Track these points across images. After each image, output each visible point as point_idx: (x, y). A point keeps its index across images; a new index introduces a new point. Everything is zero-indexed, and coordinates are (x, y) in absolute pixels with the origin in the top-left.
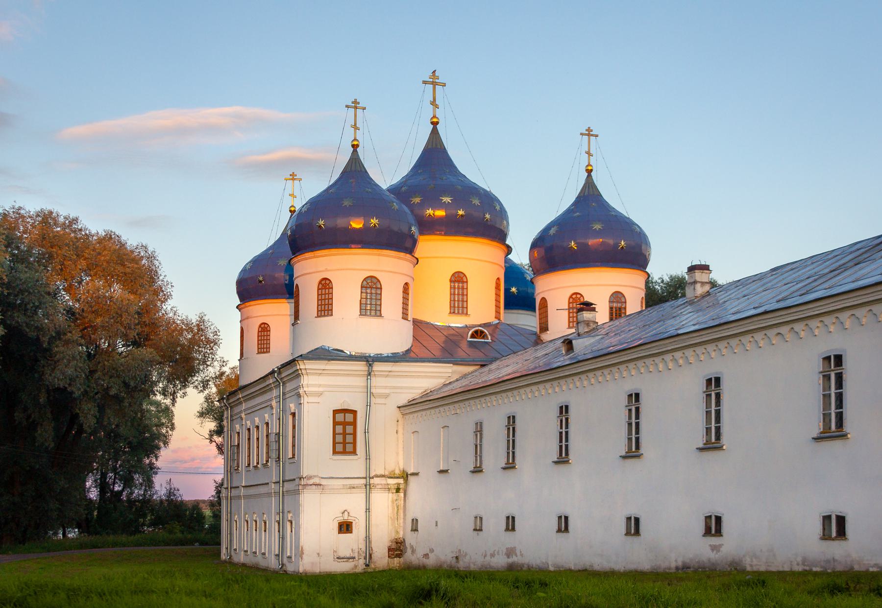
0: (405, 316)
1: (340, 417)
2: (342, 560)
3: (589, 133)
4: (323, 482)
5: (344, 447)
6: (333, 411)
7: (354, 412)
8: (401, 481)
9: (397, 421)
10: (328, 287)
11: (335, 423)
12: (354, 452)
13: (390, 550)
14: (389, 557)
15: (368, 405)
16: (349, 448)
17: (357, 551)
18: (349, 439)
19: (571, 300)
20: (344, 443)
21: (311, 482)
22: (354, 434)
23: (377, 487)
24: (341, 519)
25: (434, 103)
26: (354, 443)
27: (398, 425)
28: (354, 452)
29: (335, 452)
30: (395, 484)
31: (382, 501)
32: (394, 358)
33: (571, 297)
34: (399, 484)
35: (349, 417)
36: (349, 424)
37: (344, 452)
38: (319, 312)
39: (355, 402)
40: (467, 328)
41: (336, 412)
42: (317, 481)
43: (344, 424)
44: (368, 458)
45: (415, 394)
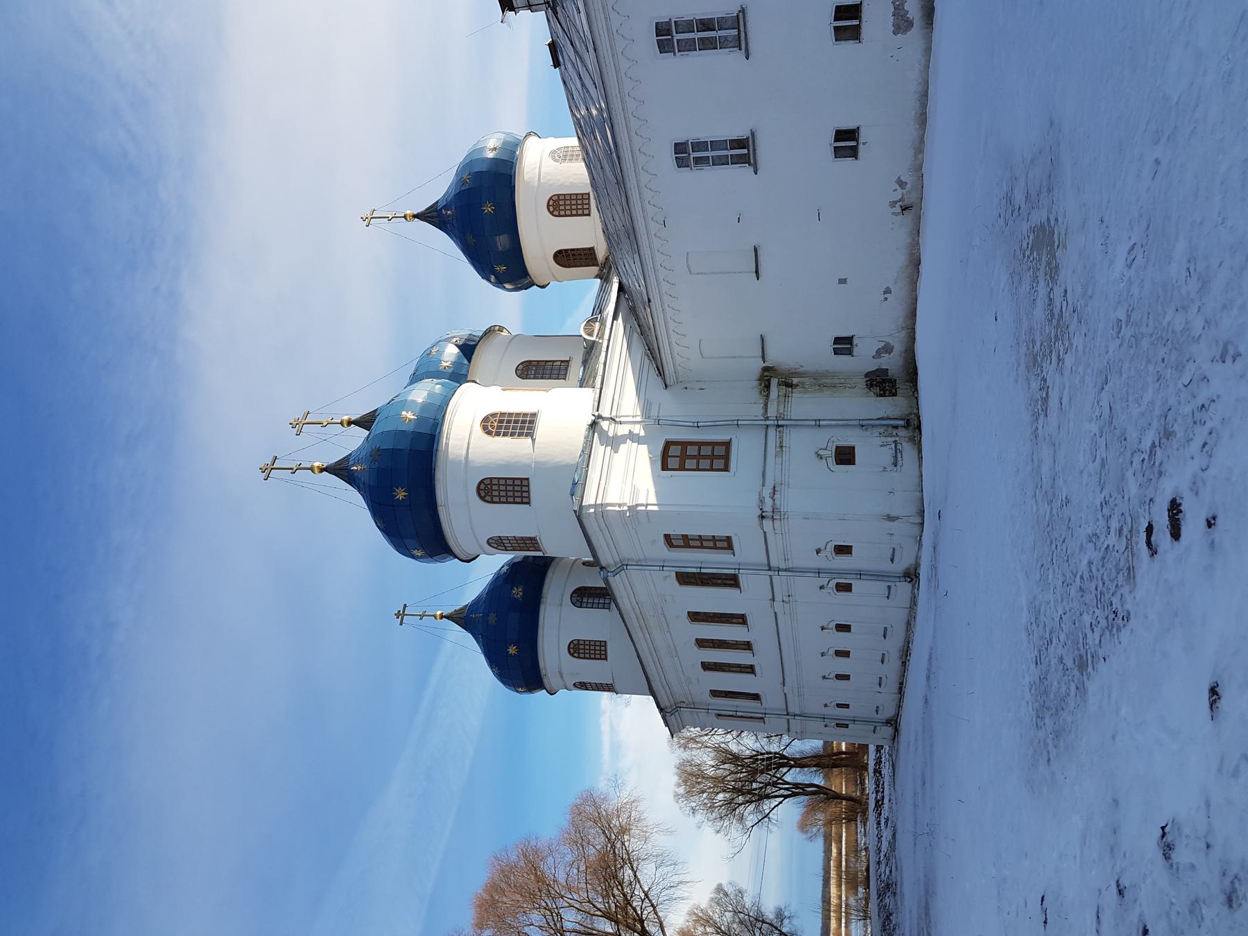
2: (899, 459)
4: (770, 483)
5: (719, 457)
6: (663, 470)
7: (668, 444)
8: (774, 382)
9: (686, 388)
10: (489, 486)
11: (682, 468)
13: (882, 395)
14: (894, 395)
16: (720, 451)
17: (883, 439)
18: (706, 451)
20: (712, 457)
21: (769, 502)
22: (700, 444)
23: (782, 411)
24: (831, 461)
26: (713, 444)
27: (692, 389)
28: (727, 445)
29: (726, 469)
30: (778, 388)
31: (802, 405)
34: (779, 384)
35: (676, 450)
36: (684, 451)
37: (727, 457)
38: (525, 500)
42: (767, 492)
43: (684, 457)
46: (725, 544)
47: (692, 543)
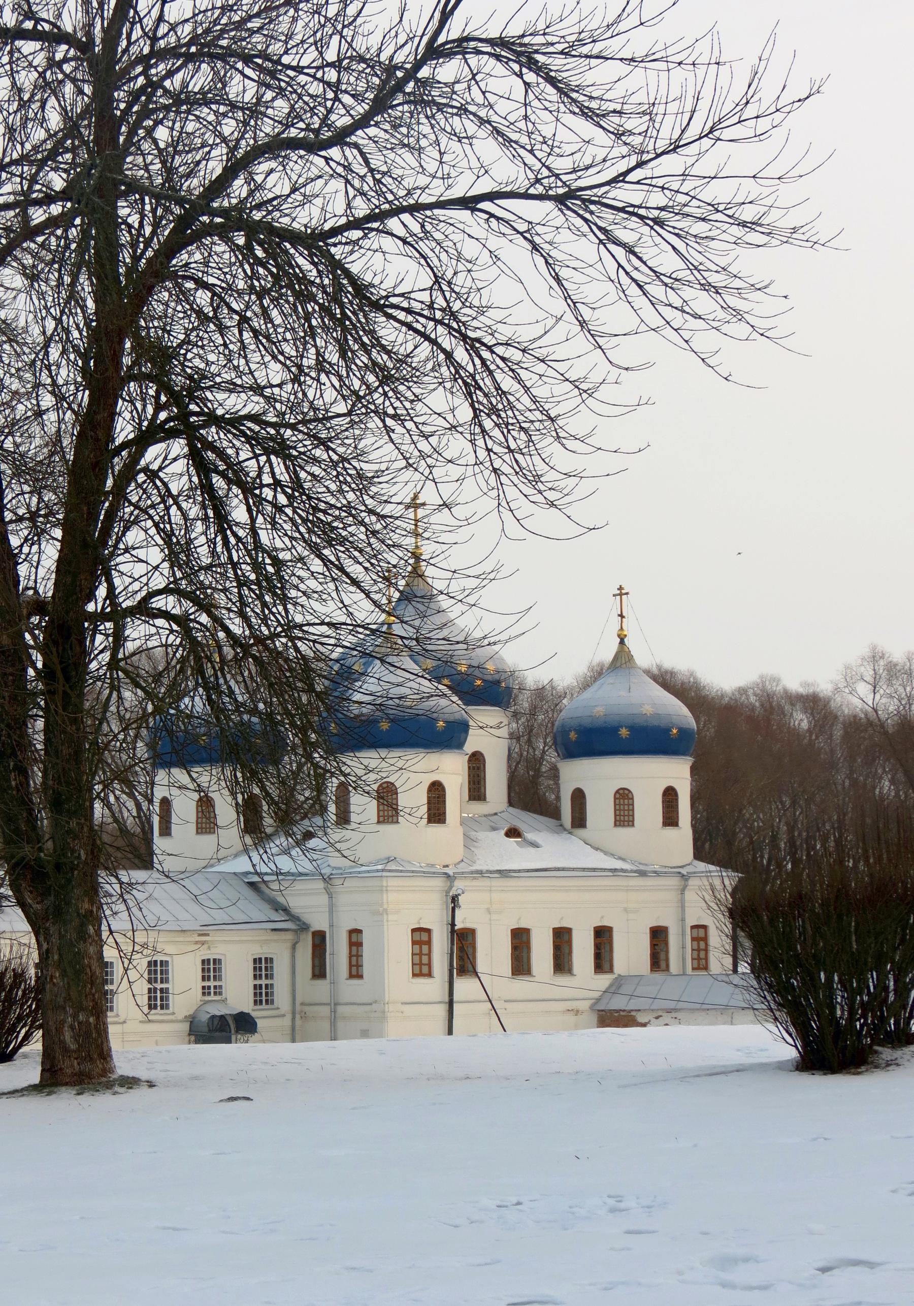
3: (621, 593)
7: (428, 931)
11: (414, 943)
12: (429, 975)
16: (425, 970)
18: (425, 959)
19: (618, 796)
20: (421, 964)
22: (429, 954)
26: (429, 965)
28: (429, 975)
29: (414, 975)
33: (617, 792)
35: (425, 937)
41: (413, 930)
46: (354, 972)
47: (354, 948)
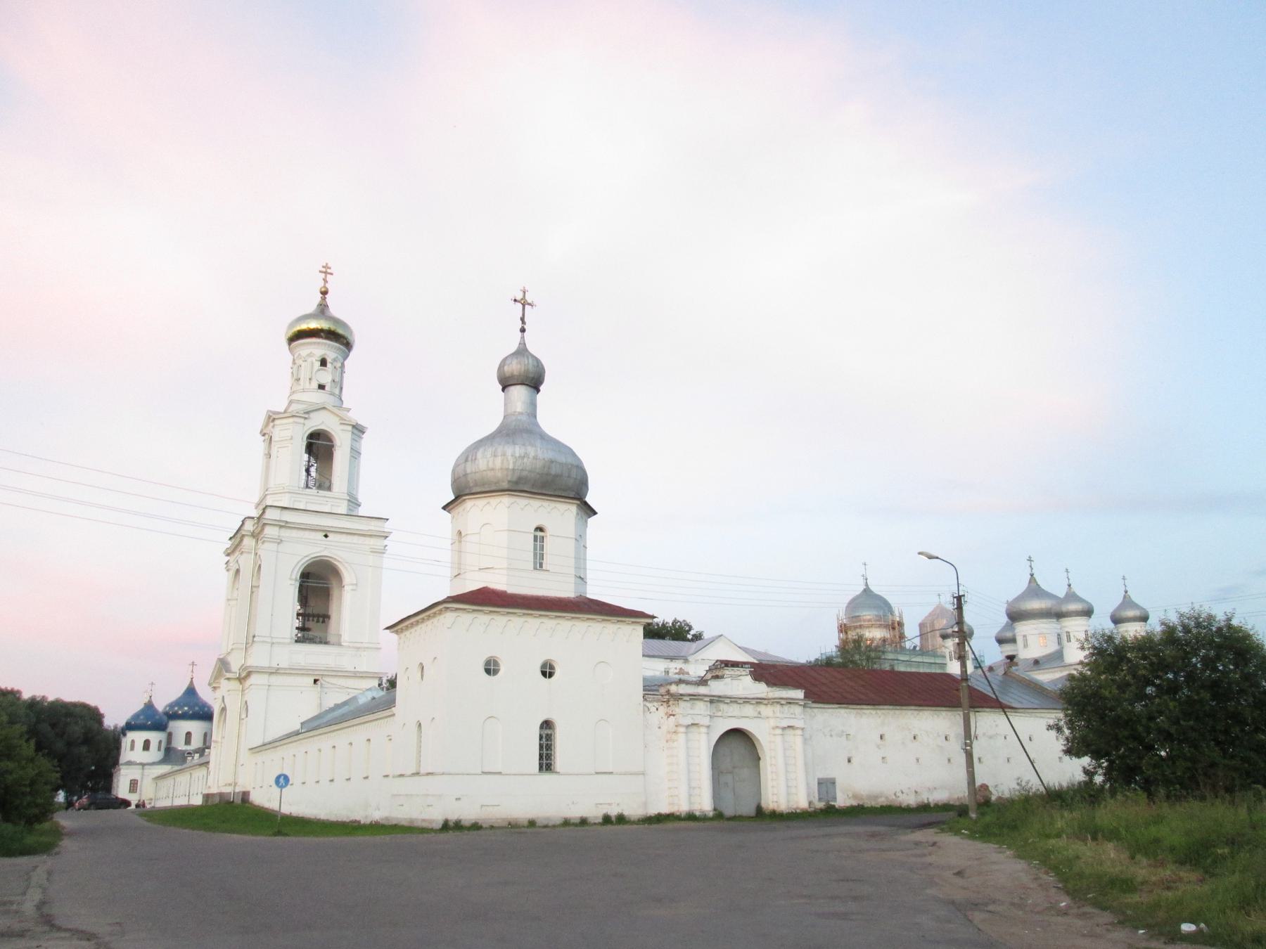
0: (159, 749)
1: (133, 782)
15: (142, 778)
25: (192, 671)
29: (130, 792)
32: (153, 764)
39: (137, 777)
40: (186, 751)
44: (140, 794)
45: (159, 774)
